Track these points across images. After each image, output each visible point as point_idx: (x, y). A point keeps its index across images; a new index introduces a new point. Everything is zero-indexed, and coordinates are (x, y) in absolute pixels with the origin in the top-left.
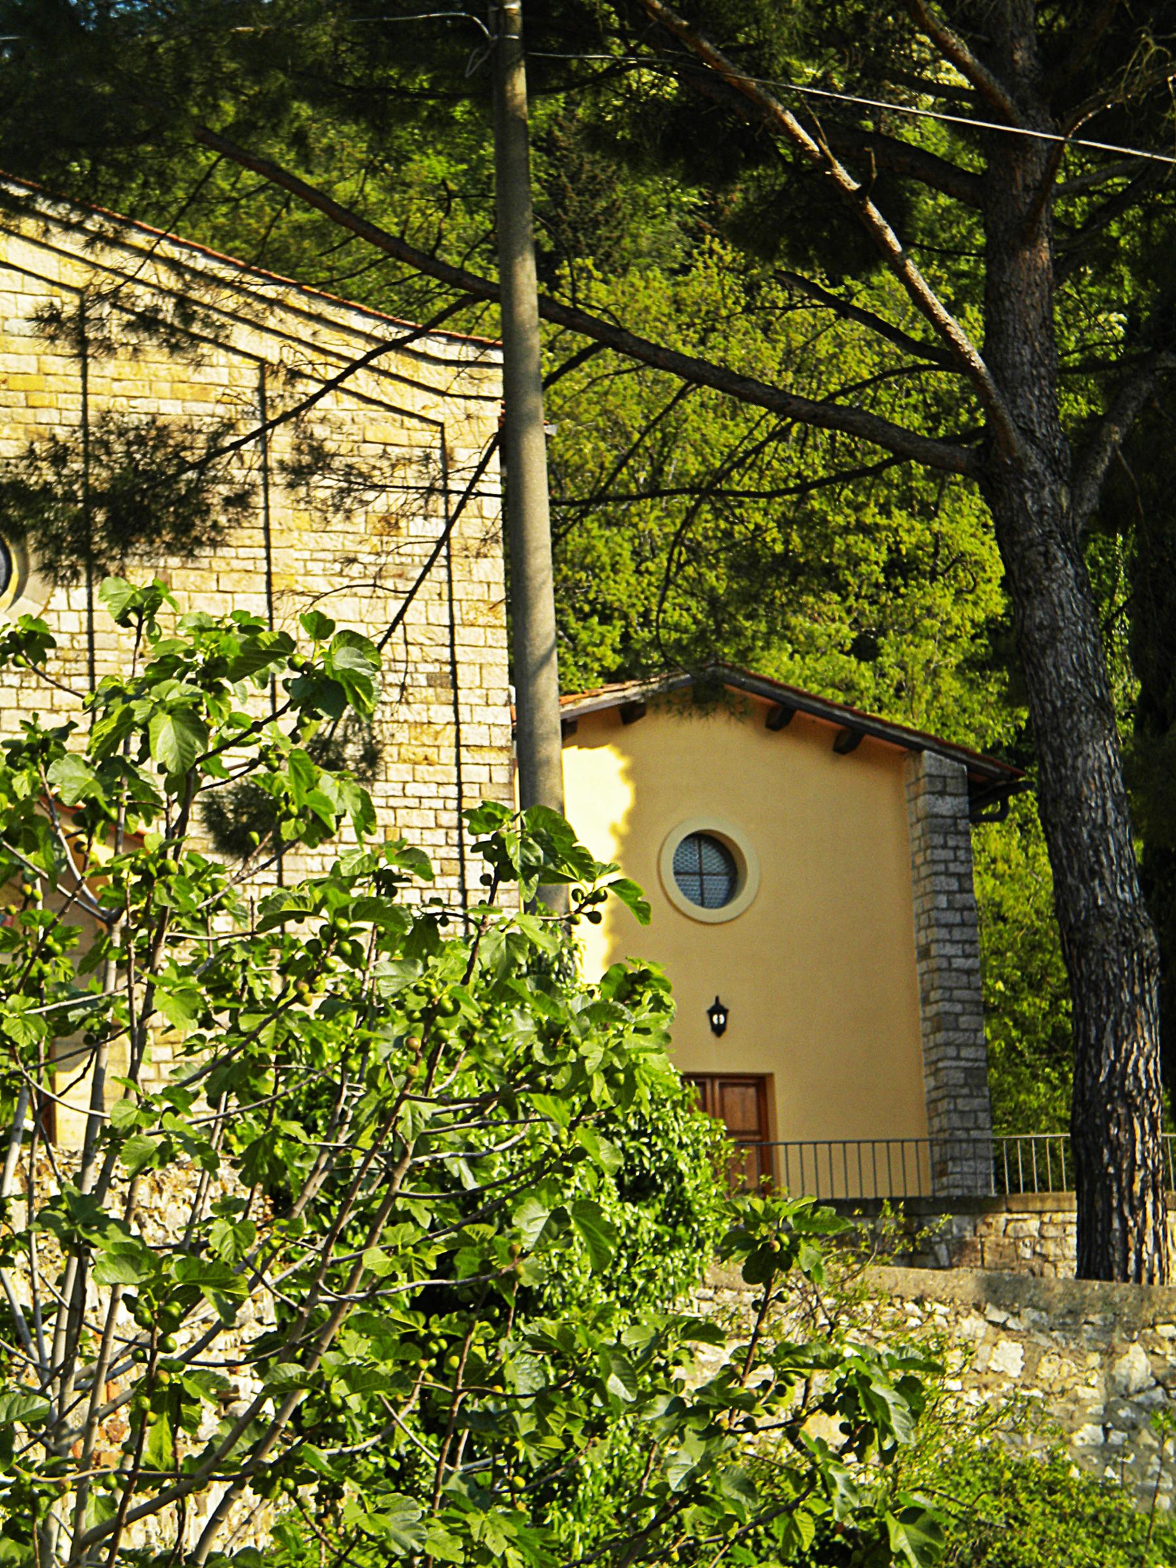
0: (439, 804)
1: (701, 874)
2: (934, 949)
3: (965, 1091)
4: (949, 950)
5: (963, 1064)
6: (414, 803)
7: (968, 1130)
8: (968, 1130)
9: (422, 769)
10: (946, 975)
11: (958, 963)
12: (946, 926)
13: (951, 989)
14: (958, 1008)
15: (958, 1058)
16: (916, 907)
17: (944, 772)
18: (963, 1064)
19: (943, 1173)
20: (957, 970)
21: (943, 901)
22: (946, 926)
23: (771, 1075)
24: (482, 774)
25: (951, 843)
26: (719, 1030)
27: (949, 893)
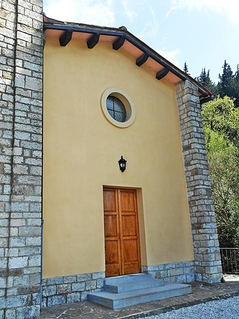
0: (5, 45)
1: (114, 110)
3: (206, 197)
4: (198, 146)
5: (205, 187)
7: (208, 211)
8: (208, 211)
10: (198, 155)
11: (201, 151)
12: (197, 138)
14: (202, 167)
15: (203, 185)
16: (184, 132)
18: (205, 187)
19: (200, 228)
20: (201, 153)
22: (197, 138)
26: (123, 169)
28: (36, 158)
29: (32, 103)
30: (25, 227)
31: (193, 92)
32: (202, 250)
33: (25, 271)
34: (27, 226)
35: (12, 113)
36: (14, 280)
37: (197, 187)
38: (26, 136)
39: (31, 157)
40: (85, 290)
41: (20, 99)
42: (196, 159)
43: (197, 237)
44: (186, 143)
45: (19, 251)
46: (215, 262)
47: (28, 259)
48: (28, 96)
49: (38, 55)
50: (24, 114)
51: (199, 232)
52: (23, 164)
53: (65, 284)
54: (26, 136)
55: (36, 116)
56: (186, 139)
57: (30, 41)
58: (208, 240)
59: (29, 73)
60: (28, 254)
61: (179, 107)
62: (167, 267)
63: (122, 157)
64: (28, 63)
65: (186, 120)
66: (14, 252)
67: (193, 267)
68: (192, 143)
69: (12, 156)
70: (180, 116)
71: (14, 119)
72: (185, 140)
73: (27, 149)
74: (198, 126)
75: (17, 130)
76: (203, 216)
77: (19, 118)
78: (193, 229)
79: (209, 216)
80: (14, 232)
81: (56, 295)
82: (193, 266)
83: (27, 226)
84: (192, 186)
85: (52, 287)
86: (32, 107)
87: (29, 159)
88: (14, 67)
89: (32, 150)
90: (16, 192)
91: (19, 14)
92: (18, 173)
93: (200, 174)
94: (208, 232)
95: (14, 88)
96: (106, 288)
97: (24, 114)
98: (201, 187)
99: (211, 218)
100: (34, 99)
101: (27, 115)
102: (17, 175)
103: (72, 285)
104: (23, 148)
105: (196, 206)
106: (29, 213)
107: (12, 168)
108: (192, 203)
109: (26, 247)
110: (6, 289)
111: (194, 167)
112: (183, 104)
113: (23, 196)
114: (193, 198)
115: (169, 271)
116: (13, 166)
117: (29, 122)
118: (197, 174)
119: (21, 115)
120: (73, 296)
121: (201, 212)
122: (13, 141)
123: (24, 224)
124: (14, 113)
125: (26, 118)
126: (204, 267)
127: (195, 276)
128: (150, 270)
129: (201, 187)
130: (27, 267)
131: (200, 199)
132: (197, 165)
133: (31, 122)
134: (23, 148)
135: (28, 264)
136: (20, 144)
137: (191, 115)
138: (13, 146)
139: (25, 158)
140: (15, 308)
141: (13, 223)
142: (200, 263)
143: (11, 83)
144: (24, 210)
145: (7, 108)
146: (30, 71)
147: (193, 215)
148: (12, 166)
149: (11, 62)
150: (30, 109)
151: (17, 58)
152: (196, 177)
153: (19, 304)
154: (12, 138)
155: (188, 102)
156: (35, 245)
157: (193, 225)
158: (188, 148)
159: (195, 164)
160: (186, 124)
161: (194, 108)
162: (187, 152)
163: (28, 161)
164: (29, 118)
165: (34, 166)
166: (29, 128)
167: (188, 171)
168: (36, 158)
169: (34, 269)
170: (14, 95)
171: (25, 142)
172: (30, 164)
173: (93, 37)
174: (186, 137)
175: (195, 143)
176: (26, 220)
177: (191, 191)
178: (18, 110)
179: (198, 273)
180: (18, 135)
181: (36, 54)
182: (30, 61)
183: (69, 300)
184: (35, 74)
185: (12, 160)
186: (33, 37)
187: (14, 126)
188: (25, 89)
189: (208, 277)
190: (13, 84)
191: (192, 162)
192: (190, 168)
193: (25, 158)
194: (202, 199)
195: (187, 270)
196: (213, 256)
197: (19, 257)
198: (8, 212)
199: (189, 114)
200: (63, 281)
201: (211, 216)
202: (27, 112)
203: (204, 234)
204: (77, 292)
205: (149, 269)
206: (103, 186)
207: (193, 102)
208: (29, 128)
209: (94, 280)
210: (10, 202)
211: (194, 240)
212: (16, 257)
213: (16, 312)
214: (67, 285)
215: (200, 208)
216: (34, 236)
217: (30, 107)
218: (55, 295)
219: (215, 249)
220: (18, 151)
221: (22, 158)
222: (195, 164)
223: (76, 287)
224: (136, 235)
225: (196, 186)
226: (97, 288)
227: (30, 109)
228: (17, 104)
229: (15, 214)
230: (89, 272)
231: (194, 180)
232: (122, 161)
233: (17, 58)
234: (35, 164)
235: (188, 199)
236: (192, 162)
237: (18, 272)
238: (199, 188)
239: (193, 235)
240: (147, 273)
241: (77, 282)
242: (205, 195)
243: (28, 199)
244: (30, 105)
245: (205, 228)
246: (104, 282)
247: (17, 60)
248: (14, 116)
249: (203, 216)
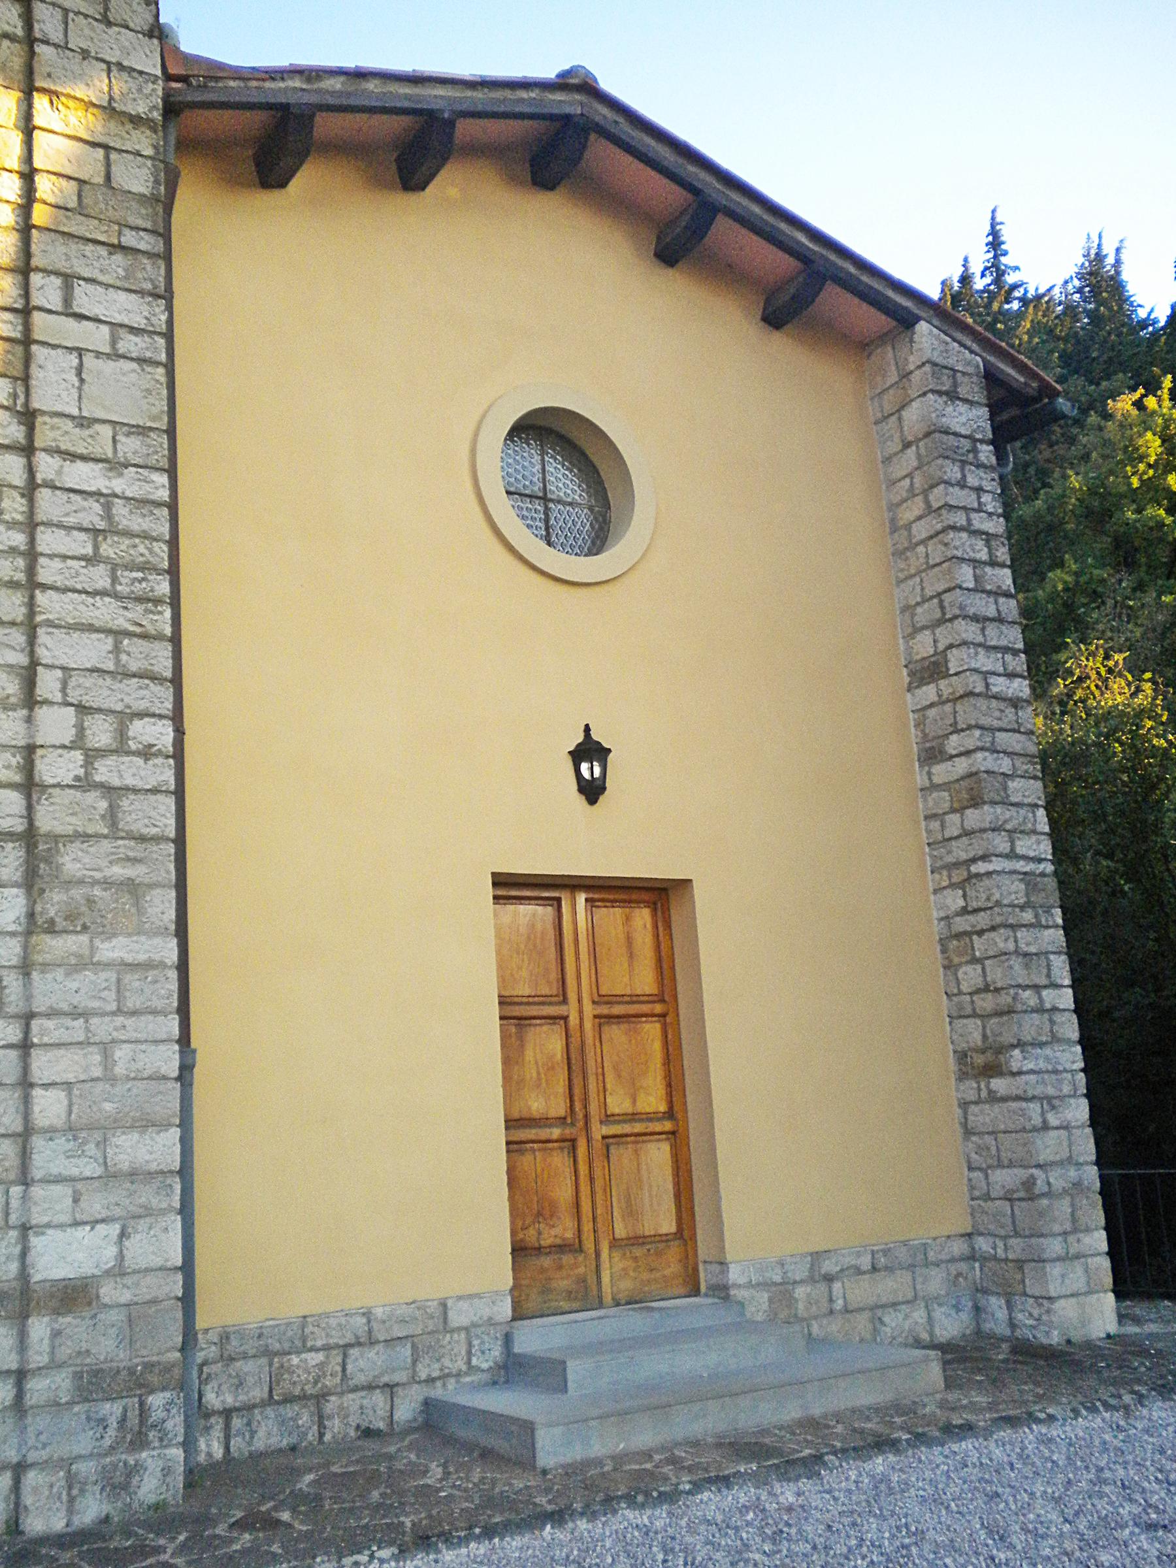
1: (545, 499)
3: (1028, 916)
4: (985, 661)
5: (1020, 865)
7: (1037, 988)
8: (1037, 988)
10: (982, 703)
11: (999, 685)
12: (975, 618)
13: (992, 730)
14: (1005, 765)
15: (1012, 855)
16: (910, 592)
17: (951, 362)
18: (1020, 865)
19: (992, 1070)
21: (966, 575)
22: (975, 618)
23: (687, 883)
25: (972, 480)
26: (592, 791)
27: (975, 563)
28: (147, 753)
29: (118, 485)
30: (100, 1086)
31: (955, 385)
32: (1003, 1178)
33: (108, 1292)
34: (112, 1080)
35: (18, 539)
36: (56, 1334)
37: (981, 867)
38: (93, 651)
39: (121, 748)
40: (414, 1380)
41: (59, 472)
42: (970, 727)
43: (982, 1116)
44: (924, 646)
45: (76, 1201)
46: (1071, 1239)
47: (123, 1235)
48: (98, 452)
49: (142, 246)
50: (81, 544)
51: (990, 1092)
52: (84, 783)
53: (313, 1349)
54: (93, 651)
55: (142, 549)
56: (924, 628)
57: (99, 179)
58: (1035, 1129)
59: (99, 337)
60: (118, 1212)
61: (887, 460)
62: (829, 1266)
63: (587, 729)
64: (90, 288)
65: (921, 530)
66: (49, 1202)
67: (963, 1267)
68: (951, 646)
69: (30, 750)
70: (893, 507)
71: (31, 571)
72: (916, 630)
73: (99, 710)
74: (983, 555)
75: (50, 624)
76: (1010, 1011)
77: (57, 564)
78: (962, 1076)
79: (1040, 1010)
80: (49, 1107)
81: (270, 1401)
82: (962, 1259)
83: (112, 1080)
84: (957, 865)
85: (248, 1367)
86: (120, 510)
87: (111, 761)
89: (125, 717)
90: (52, 922)
91: (40, 49)
92: (59, 829)
93: (994, 803)
94: (1038, 1091)
96: (514, 1369)
98: (996, 865)
99: (1052, 1022)
100: (126, 466)
101: (96, 547)
102: (56, 838)
103: (345, 1356)
104: (82, 709)
105: (974, 960)
106: (120, 1020)
107: (30, 808)
108: (955, 944)
109: (110, 1176)
110: (20, 1376)
111: (961, 766)
112: (907, 445)
113: (84, 939)
114: (962, 924)
115: (837, 1286)
116: (35, 797)
117: (104, 583)
118: (976, 802)
119: (63, 550)
120: (354, 1408)
121: (997, 990)
122: (29, 676)
123: (97, 1072)
124: (32, 541)
125: (91, 560)
126: (1020, 1264)
127: (977, 1309)
128: (742, 1281)
129: (996, 865)
130: (119, 1270)
131: (993, 928)
132: (979, 755)
133: (115, 580)
134: (82, 709)
135: (121, 1256)
136: (64, 690)
137: (946, 505)
138: (31, 700)
139: (92, 756)
140: (66, 1463)
141: (43, 1066)
142: (1000, 1244)
143: (15, 396)
144: (96, 1004)
146: (105, 329)
147: (960, 1007)
148: (29, 797)
150: (108, 516)
151: (38, 269)
152: (973, 817)
153: (84, 1443)
154: (23, 660)
155: (928, 435)
156: (153, 1167)
157: (962, 1056)
158: (930, 670)
159: (967, 753)
160: (921, 549)
161: (963, 463)
162: (929, 693)
163: (105, 771)
164: (107, 561)
165: (135, 791)
166: (106, 612)
167: (934, 787)
168: (147, 753)
169: (150, 1280)
170: (28, 450)
171: (89, 681)
172: (116, 782)
173: (415, 137)
174: (924, 614)
175: (965, 643)
176: (106, 1049)
177: (952, 886)
178: (48, 524)
179: (985, 1292)
180: (51, 647)
181: (129, 238)
182: (101, 278)
183: (335, 1426)
184: (131, 344)
185: (28, 767)
186: (114, 156)
187: (31, 604)
188: (83, 422)
189: (1036, 1313)
190: (21, 400)
191: (954, 743)
192: (942, 772)
193: (92, 756)
194: (1006, 926)
195: (935, 1282)
196: (1064, 1207)
197: (76, 1224)
198: (15, 1016)
199: (937, 496)
200: (304, 1340)
201: (1055, 1009)
202: (95, 532)
203: (1018, 1098)
204: (370, 1387)
205: (735, 1275)
206: (493, 874)
207: (956, 434)
208: (106, 612)
209: (459, 1329)
210: (25, 968)
211: (968, 1132)
212: (61, 1226)
213: (71, 1480)
214: (320, 1357)
215: (996, 975)
216: (147, 1124)
217: (107, 507)
218: (263, 1404)
219: (1072, 1173)
220: (55, 724)
221: (78, 756)
222: (967, 753)
223: (366, 1364)
224: (670, 1114)
225: (974, 860)
226: (471, 1368)
227: (108, 516)
228: (43, 495)
229: (50, 1024)
230: (429, 1291)
231: (967, 833)
232: (589, 750)
233: (38, 269)
234: (140, 784)
235: (937, 928)
236: (954, 743)
237: (73, 1296)
238: (989, 874)
239: (964, 1105)
240: (727, 1298)
241: (372, 1343)
242: (1022, 908)
243: (113, 950)
244: (106, 499)
245: (1020, 1073)
246: (508, 1339)
247: (36, 279)
248: (32, 555)
249: (1010, 1011)
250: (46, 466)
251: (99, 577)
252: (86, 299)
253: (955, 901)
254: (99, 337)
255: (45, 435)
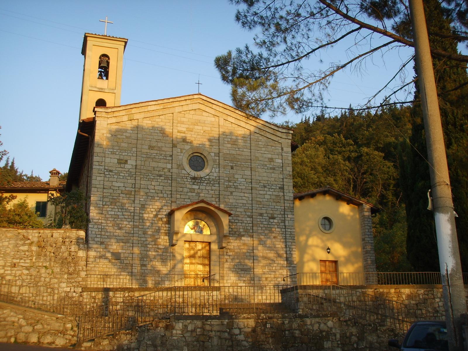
0: (281, 210)
2: (366, 239)
4: (368, 239)
6: (276, 210)
9: (278, 204)
11: (370, 241)
21: (367, 230)
23: (337, 261)
24: (288, 205)
44: (363, 237)
50: (289, 236)
88: (285, 218)
95: (285, 226)
97: (289, 236)
145: (283, 234)
149: (283, 216)
166: (291, 240)
170: (285, 228)
185: (286, 252)
192: (365, 250)
208: (291, 240)
228: (287, 232)
248: (286, 236)
250: (287, 230)
251: (290, 238)
252: (289, 216)
253: (365, 263)
254: (289, 219)
255: (287, 227)
